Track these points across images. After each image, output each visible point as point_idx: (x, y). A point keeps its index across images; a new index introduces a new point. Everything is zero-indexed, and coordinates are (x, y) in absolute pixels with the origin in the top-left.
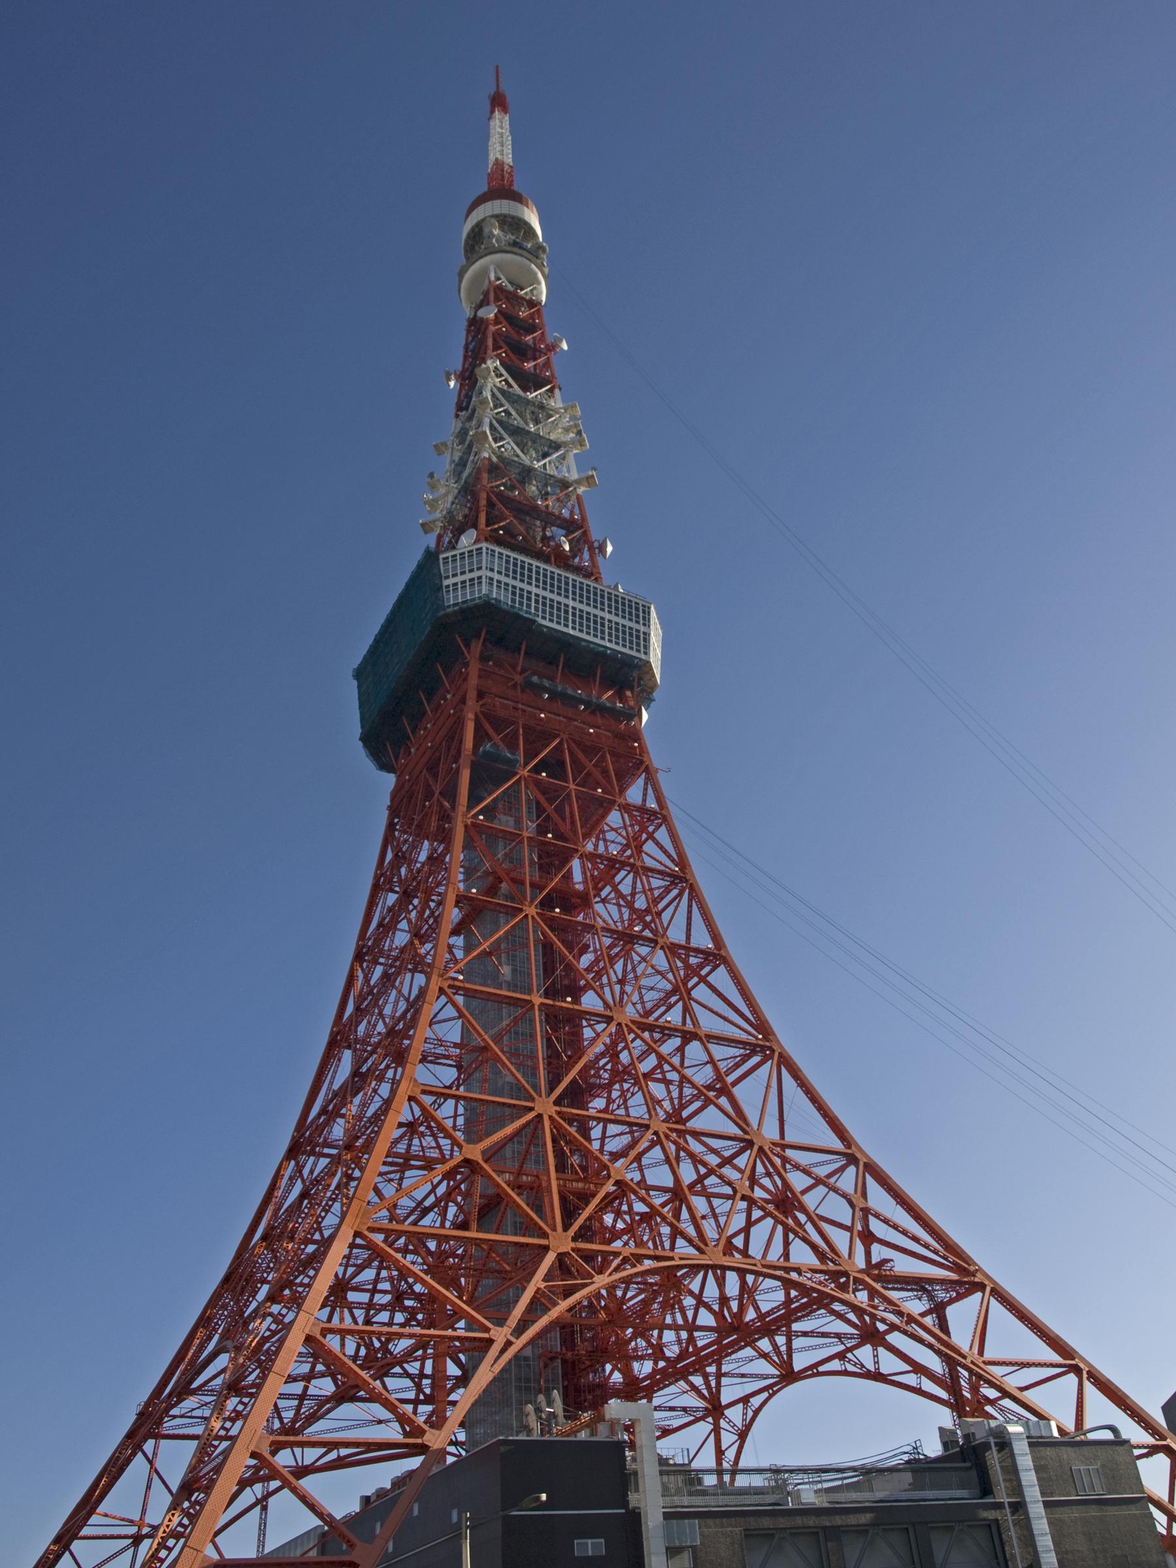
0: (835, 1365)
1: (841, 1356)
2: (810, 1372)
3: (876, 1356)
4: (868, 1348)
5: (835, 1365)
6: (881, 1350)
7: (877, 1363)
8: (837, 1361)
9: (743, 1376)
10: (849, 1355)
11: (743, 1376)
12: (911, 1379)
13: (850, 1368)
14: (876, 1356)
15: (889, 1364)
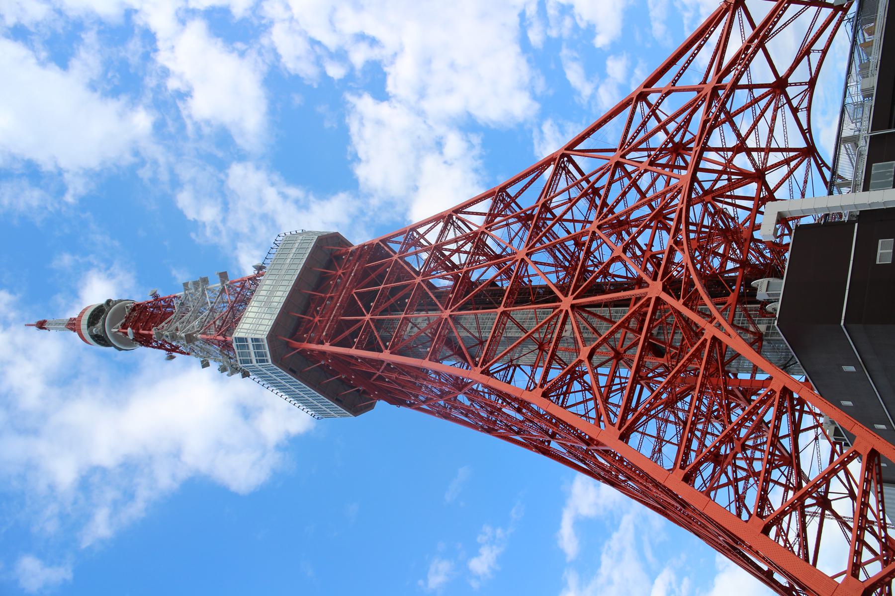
0: (802, 116)
1: (795, 111)
2: (807, 134)
3: (795, 84)
4: (788, 89)
5: (802, 116)
6: (790, 80)
7: (801, 84)
8: (798, 114)
9: (806, 182)
10: (795, 103)
11: (806, 182)
12: (815, 57)
13: (805, 104)
14: (795, 84)
15: (802, 74)
